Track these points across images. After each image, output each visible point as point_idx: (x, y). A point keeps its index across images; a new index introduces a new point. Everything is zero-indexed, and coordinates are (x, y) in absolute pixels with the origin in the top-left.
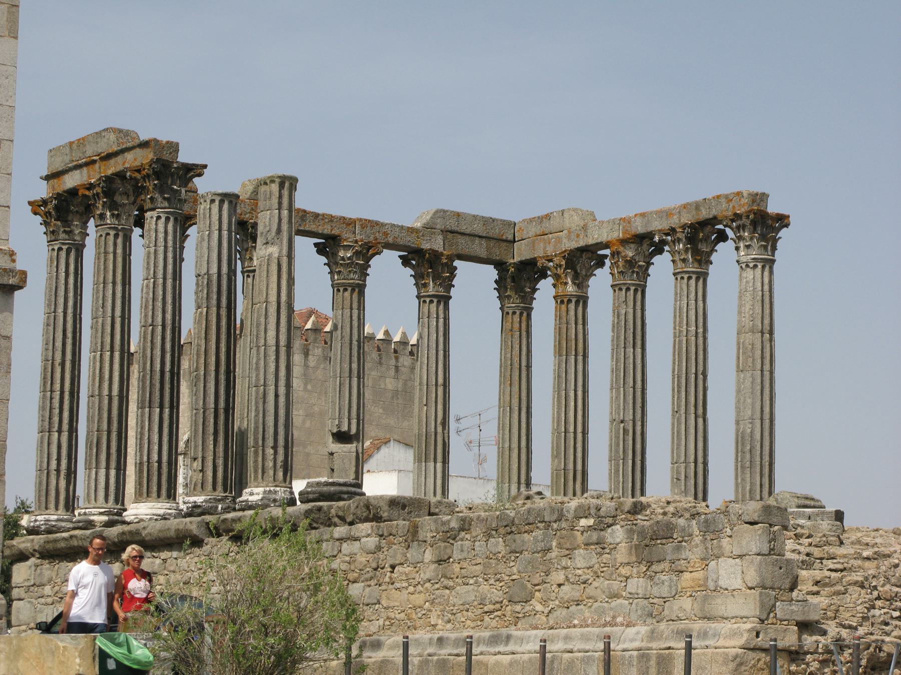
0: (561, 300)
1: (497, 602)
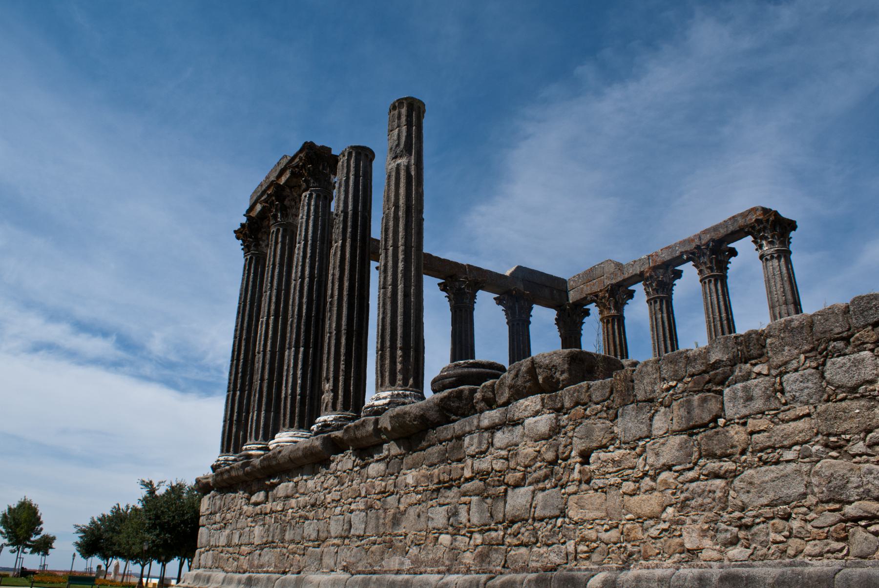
0: (606, 321)
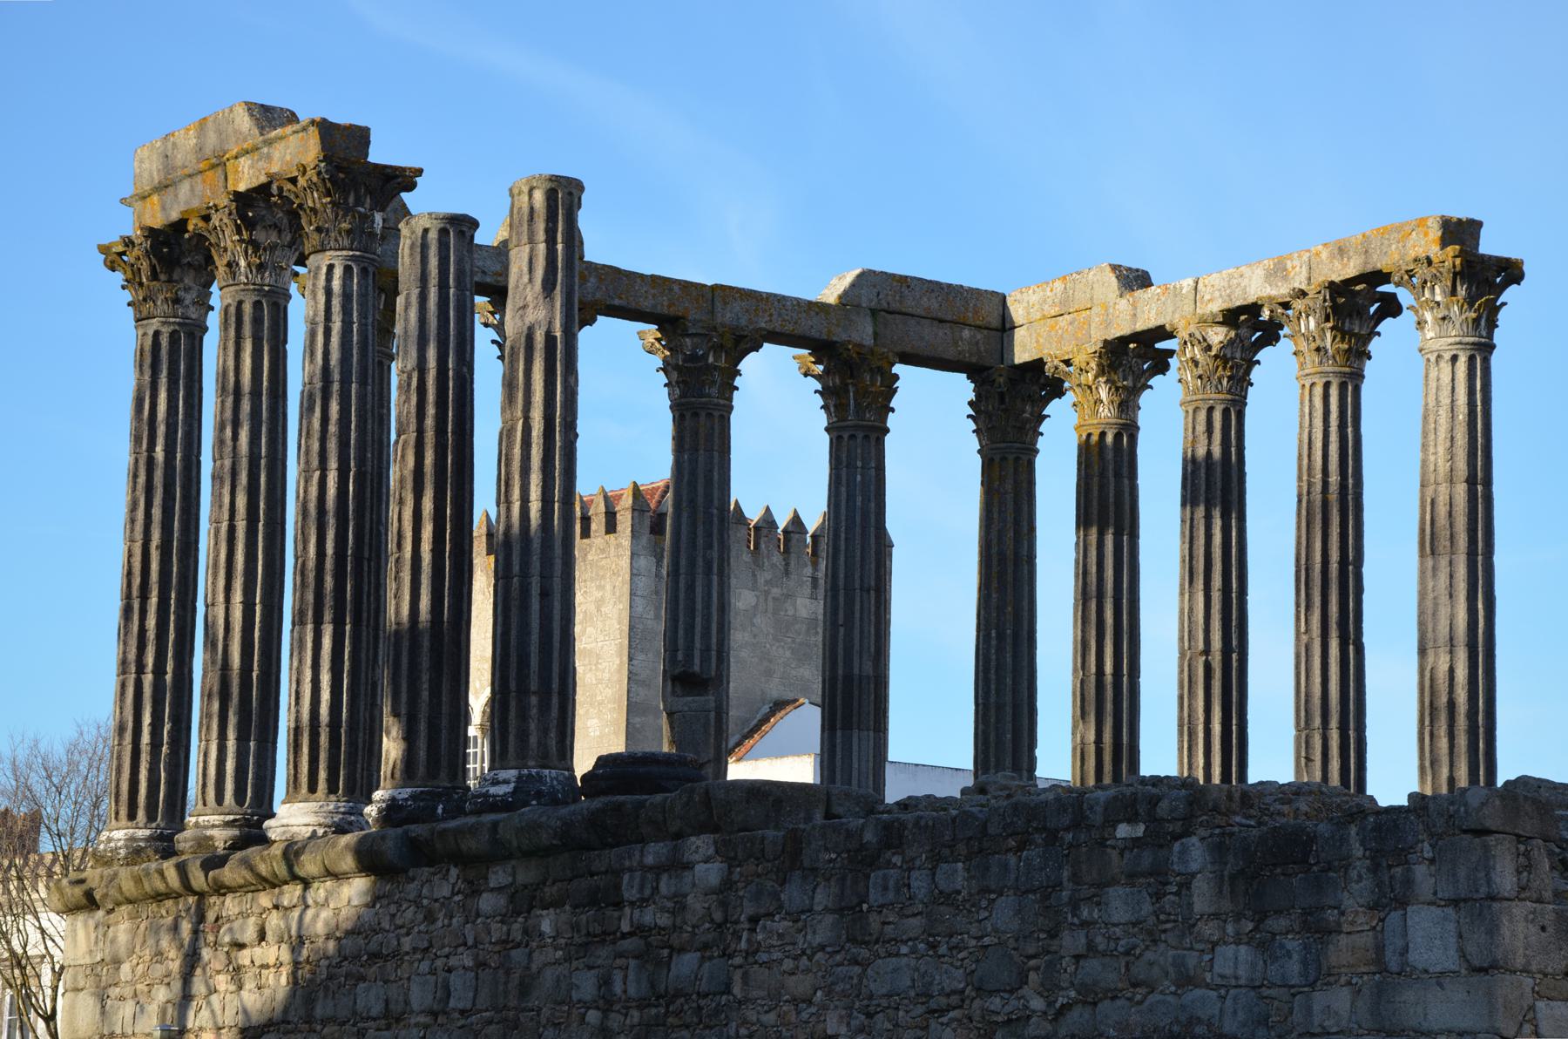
1: (954, 992)
